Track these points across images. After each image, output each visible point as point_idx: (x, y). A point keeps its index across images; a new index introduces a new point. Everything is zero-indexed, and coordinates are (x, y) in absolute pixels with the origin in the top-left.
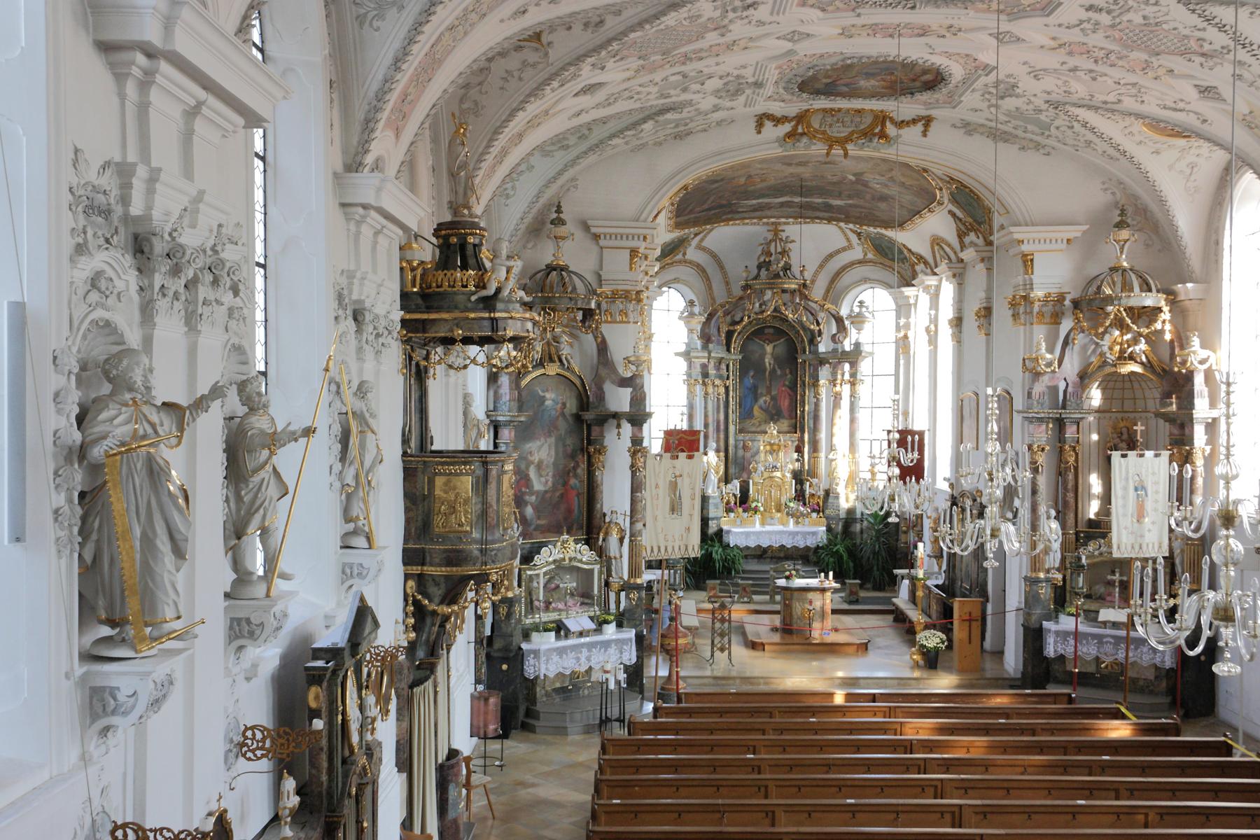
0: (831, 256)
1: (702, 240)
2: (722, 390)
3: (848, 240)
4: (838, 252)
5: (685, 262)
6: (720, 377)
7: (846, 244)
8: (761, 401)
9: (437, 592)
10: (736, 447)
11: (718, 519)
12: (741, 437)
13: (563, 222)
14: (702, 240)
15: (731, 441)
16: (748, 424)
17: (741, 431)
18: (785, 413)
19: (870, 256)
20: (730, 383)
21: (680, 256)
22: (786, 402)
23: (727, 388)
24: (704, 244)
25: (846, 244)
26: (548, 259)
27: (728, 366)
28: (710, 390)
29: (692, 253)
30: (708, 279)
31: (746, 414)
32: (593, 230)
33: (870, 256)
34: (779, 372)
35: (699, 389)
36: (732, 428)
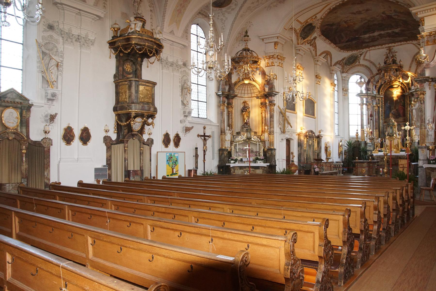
1: (364, 57)
2: (377, 108)
6: (376, 104)
8: (392, 111)
9: (124, 120)
10: (383, 128)
11: (371, 151)
12: (385, 124)
13: (248, 36)
14: (364, 57)
15: (381, 125)
17: (385, 122)
18: (402, 115)
21: (357, 63)
23: (379, 107)
24: (366, 58)
26: (244, 47)
27: (379, 99)
29: (362, 62)
30: (371, 71)
32: (261, 37)
34: (399, 100)
35: (365, 106)
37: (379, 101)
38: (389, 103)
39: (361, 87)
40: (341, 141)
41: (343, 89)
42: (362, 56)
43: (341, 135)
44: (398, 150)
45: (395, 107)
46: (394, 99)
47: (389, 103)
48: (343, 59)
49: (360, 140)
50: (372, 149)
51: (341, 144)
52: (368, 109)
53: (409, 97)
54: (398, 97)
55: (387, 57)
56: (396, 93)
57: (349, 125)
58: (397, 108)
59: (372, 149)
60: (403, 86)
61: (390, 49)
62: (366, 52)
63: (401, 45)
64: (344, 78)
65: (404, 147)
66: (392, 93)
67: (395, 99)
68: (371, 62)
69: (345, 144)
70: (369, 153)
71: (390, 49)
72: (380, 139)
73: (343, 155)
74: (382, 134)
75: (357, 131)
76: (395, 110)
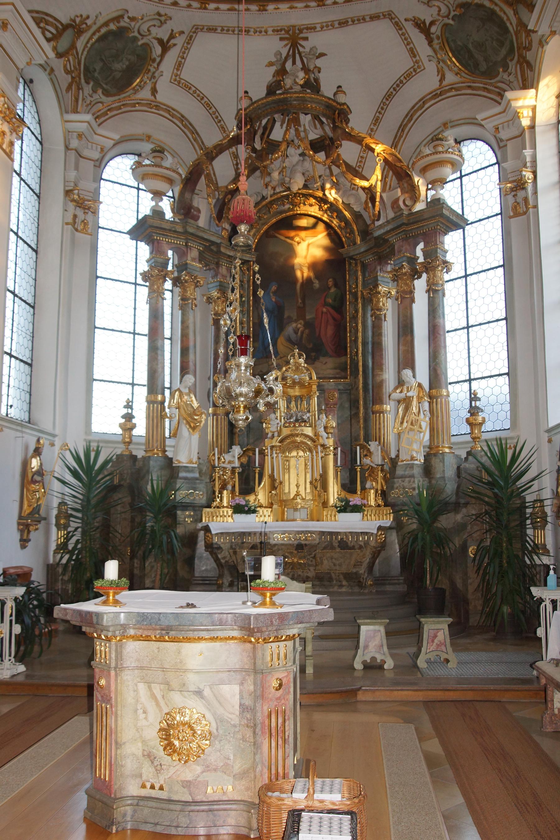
0: (389, 97)
1: (179, 66)
3: (413, 53)
4: (398, 85)
5: (155, 106)
7: (407, 63)
8: (290, 330)
14: (179, 66)
19: (450, 78)
21: (145, 94)
22: (330, 331)
24: (185, 75)
25: (407, 63)
33: (450, 78)
34: (317, 284)
38: (275, 293)
39: (158, 195)
40: (37, 452)
41: (68, 193)
42: (172, 56)
43: (45, 421)
44: (325, 504)
45: (301, 314)
46: (299, 274)
47: (275, 293)
48: (76, 27)
49: (140, 454)
50: (200, 496)
51: (35, 463)
52: (184, 304)
53: (364, 267)
54: (313, 266)
55: (282, 72)
56: (309, 248)
57: (90, 380)
58: (308, 317)
59: (200, 496)
60: (335, 223)
61: (293, 37)
62: (190, 40)
63: (343, 23)
64: (74, 143)
65: (354, 492)
66: (291, 252)
68: (208, 106)
69: (56, 463)
71: (293, 37)
72: (237, 450)
73: (54, 529)
75: (129, 405)
76: (300, 325)
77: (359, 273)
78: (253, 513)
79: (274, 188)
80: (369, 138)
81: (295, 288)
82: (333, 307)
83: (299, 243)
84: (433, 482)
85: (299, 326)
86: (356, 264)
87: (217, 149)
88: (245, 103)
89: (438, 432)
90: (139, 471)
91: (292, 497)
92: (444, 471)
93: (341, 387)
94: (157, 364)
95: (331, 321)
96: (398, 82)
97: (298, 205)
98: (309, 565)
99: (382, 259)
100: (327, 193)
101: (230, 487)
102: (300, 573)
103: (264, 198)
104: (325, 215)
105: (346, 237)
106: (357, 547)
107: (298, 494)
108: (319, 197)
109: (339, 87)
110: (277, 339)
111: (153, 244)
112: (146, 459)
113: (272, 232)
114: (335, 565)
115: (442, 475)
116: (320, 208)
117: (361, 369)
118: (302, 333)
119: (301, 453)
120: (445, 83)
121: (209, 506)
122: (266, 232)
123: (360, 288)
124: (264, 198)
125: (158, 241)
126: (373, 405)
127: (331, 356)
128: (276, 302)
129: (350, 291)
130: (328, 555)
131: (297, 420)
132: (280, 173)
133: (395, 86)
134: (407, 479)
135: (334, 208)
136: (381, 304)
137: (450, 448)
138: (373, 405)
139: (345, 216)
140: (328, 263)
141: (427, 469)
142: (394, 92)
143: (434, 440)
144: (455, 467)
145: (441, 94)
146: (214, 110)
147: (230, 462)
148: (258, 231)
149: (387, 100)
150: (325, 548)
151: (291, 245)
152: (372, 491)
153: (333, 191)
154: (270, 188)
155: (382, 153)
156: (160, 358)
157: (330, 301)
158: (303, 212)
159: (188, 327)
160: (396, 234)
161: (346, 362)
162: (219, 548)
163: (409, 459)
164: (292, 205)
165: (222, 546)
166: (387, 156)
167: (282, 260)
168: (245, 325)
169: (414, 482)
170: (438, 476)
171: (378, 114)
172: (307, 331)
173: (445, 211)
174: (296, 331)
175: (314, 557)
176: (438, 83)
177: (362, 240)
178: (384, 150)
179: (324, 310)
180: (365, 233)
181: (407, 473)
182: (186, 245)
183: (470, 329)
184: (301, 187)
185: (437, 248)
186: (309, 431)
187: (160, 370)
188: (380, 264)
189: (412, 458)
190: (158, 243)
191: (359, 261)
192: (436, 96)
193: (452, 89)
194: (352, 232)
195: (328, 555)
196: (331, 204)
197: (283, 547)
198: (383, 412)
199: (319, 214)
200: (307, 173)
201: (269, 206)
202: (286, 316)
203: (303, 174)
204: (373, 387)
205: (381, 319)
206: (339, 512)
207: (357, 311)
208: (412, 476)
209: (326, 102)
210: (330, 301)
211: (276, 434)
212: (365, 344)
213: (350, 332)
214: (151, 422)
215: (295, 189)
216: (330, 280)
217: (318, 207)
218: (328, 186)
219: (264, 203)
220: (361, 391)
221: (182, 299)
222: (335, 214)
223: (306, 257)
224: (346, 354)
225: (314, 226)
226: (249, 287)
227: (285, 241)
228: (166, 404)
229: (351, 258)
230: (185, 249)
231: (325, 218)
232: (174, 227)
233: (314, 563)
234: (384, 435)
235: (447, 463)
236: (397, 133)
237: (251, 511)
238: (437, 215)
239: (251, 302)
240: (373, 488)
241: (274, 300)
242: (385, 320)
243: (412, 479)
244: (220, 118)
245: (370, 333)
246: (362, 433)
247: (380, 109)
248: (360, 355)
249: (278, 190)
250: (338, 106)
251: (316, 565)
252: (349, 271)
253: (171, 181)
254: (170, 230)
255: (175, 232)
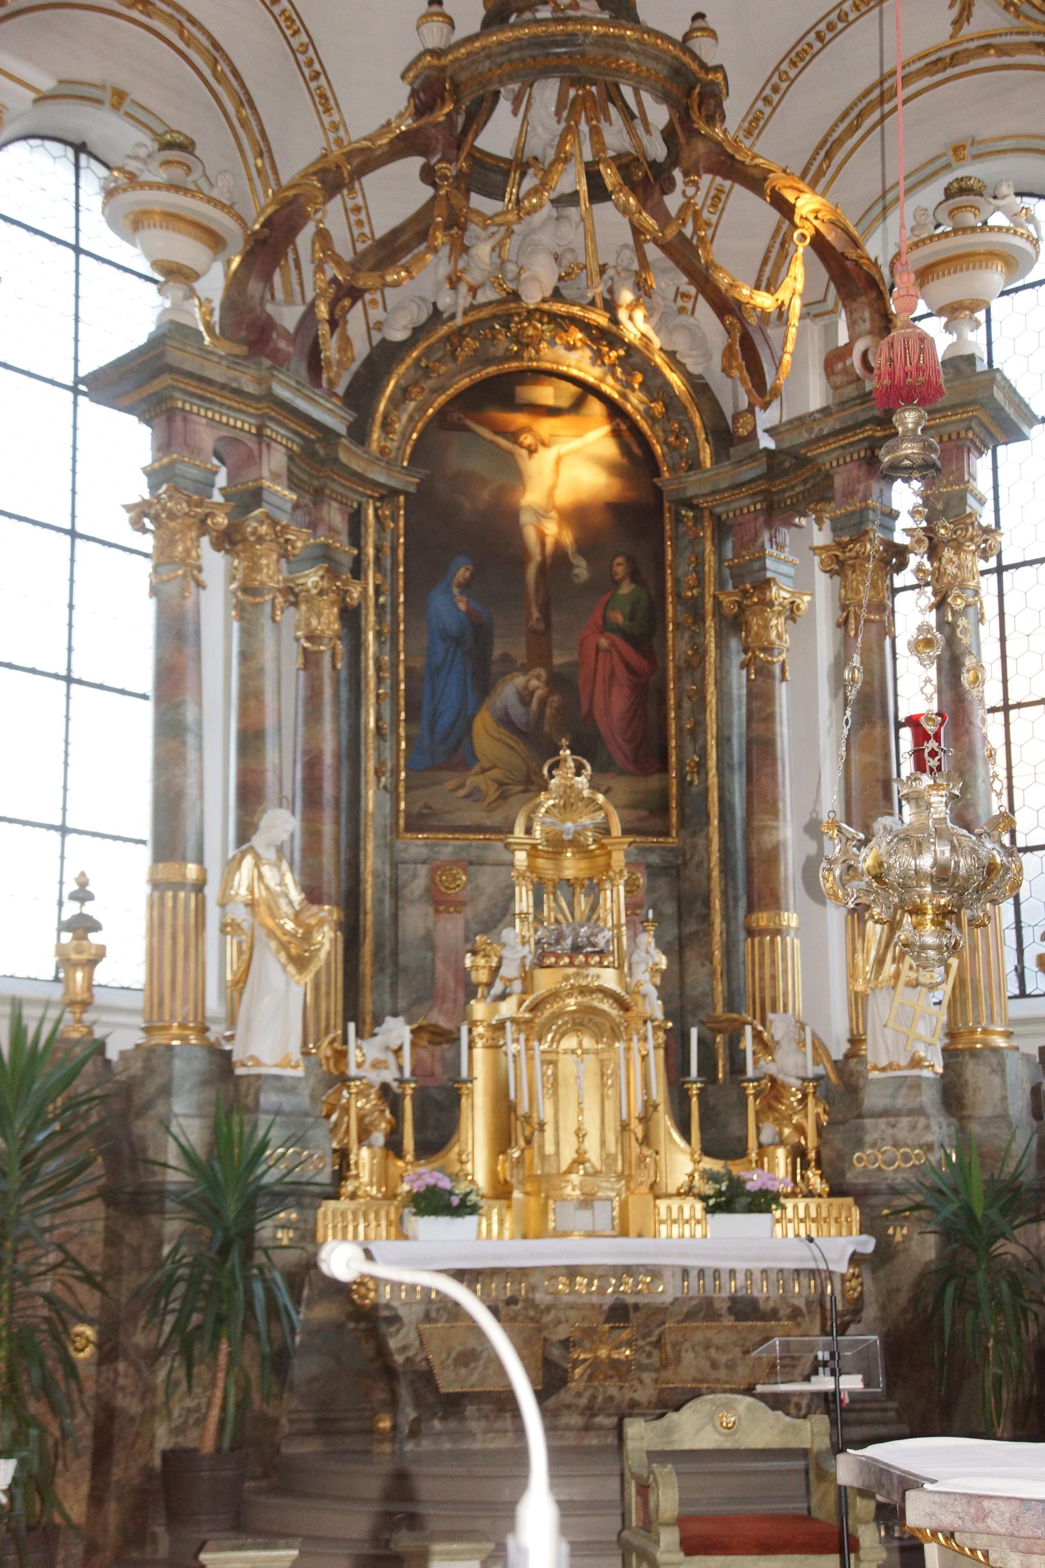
8: (507, 692)
12: (416, 845)
16: (448, 792)
17: (416, 823)
20: (365, 590)
23: (351, 617)
27: (355, 520)
28: (271, 571)
31: (439, 749)
34: (582, 570)
36: (371, 797)
37: (356, 538)
46: (531, 535)
53: (722, 529)
56: (567, 467)
58: (558, 660)
60: (635, 402)
67: (546, 532)
70: (276, 1231)
72: (398, 1031)
74: (375, 965)
76: (536, 682)
77: (709, 547)
78: (471, 1214)
79: (473, 290)
80: (780, 174)
81: (522, 579)
82: (627, 636)
83: (532, 451)
84: (975, 1128)
85: (534, 683)
86: (697, 520)
87: (356, 162)
88: (435, 36)
89: (976, 992)
90: (128, 1090)
91: (564, 1167)
92: (1004, 1098)
93: (654, 859)
94: (185, 775)
95: (621, 674)
96: (833, 17)
97: (534, 343)
98: (642, 1368)
99: (777, 511)
100: (623, 315)
101: (379, 1138)
102: (613, 1391)
103: (436, 315)
104: (610, 380)
105: (666, 443)
106: (784, 1311)
107: (580, 1160)
108: (598, 328)
109: (699, 16)
110: (473, 716)
111: (170, 420)
112: (152, 1057)
113: (456, 416)
114: (714, 1365)
115: (999, 1110)
116: (598, 357)
117: (714, 810)
118: (543, 702)
119: (588, 1043)
120: (967, 30)
121: (336, 1196)
122: (442, 413)
123: (711, 589)
124: (436, 315)
125: (186, 415)
126: (750, 909)
127: (622, 772)
128: (469, 613)
129: (678, 595)
130: (699, 1336)
131: (576, 949)
132: (493, 250)
133: (822, 27)
134: (905, 1121)
135: (636, 359)
136: (773, 635)
137: (1008, 1035)
138: (750, 909)
139: (667, 384)
140: (617, 511)
141: (953, 1095)
142: (818, 45)
143: (964, 1013)
144: (1028, 1088)
145: (954, 60)
146: (306, 39)
147: (376, 1065)
148: (421, 409)
149: (794, 64)
150: (690, 1316)
151: (511, 454)
152: (781, 1153)
153: (639, 314)
154: (463, 288)
155: (811, 217)
156: (191, 755)
157: (618, 618)
158: (548, 365)
159: (261, 671)
160: (842, 447)
161: (664, 793)
162: (395, 1319)
163: (904, 1062)
164: (518, 343)
165: (402, 1312)
166: (822, 229)
167: (485, 495)
168: (387, 675)
169: (927, 1127)
170: (987, 1111)
171: (760, 104)
172: (555, 699)
173: (998, 394)
174: (525, 697)
175: (658, 1344)
176: (949, 29)
177: (718, 456)
178: (817, 211)
179: (604, 642)
180: (726, 437)
181: (900, 1102)
182: (260, 434)
183: (1013, 713)
184: (548, 293)
185: (966, 490)
186: (609, 978)
187: (192, 792)
188: (769, 524)
189: (916, 1062)
190: (185, 419)
191: (706, 513)
192: (936, 65)
193: (987, 47)
194: (686, 429)
195: (699, 1336)
196: (630, 347)
197: (571, 1313)
198: (777, 931)
199: (591, 374)
200: (569, 257)
201: (455, 341)
202: (496, 653)
203: (557, 258)
204: (749, 861)
205: (770, 675)
206: (710, 1210)
207: (701, 653)
208: (918, 1112)
209: (676, 58)
210: (618, 618)
211: (517, 986)
212: (724, 741)
213: (679, 706)
214: (168, 943)
215: (532, 297)
216: (620, 560)
217: (588, 353)
218: (627, 296)
219: (443, 331)
220: (715, 874)
221: (246, 590)
222: (639, 377)
223: (552, 489)
224: (664, 768)
225: (577, 406)
226: (395, 564)
227: (492, 442)
228: (212, 892)
229: (688, 503)
230: (252, 444)
231: (610, 388)
232: (235, 380)
233: (655, 1359)
234: (785, 994)
235: (1010, 1078)
236: (810, 163)
237: (465, 1208)
238: (974, 402)
239: (401, 610)
240: (782, 1143)
241: (462, 606)
242: (783, 678)
243: (922, 1121)
244: (317, 67)
245: (738, 715)
246: (720, 988)
247: (768, 91)
248: (713, 772)
249: (482, 297)
250: (702, 75)
251: (664, 1365)
252: (675, 539)
253: (215, 241)
254: (223, 387)
255: (238, 392)
